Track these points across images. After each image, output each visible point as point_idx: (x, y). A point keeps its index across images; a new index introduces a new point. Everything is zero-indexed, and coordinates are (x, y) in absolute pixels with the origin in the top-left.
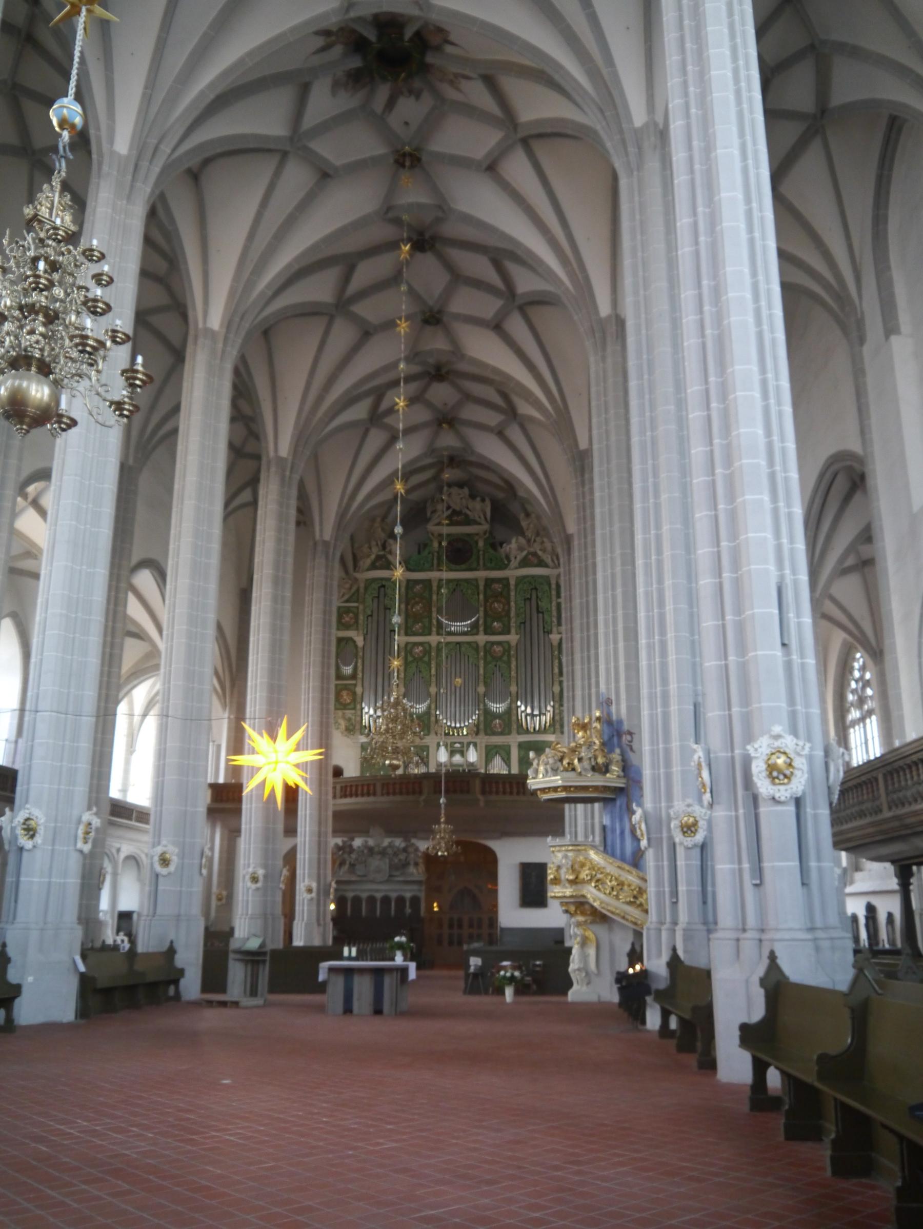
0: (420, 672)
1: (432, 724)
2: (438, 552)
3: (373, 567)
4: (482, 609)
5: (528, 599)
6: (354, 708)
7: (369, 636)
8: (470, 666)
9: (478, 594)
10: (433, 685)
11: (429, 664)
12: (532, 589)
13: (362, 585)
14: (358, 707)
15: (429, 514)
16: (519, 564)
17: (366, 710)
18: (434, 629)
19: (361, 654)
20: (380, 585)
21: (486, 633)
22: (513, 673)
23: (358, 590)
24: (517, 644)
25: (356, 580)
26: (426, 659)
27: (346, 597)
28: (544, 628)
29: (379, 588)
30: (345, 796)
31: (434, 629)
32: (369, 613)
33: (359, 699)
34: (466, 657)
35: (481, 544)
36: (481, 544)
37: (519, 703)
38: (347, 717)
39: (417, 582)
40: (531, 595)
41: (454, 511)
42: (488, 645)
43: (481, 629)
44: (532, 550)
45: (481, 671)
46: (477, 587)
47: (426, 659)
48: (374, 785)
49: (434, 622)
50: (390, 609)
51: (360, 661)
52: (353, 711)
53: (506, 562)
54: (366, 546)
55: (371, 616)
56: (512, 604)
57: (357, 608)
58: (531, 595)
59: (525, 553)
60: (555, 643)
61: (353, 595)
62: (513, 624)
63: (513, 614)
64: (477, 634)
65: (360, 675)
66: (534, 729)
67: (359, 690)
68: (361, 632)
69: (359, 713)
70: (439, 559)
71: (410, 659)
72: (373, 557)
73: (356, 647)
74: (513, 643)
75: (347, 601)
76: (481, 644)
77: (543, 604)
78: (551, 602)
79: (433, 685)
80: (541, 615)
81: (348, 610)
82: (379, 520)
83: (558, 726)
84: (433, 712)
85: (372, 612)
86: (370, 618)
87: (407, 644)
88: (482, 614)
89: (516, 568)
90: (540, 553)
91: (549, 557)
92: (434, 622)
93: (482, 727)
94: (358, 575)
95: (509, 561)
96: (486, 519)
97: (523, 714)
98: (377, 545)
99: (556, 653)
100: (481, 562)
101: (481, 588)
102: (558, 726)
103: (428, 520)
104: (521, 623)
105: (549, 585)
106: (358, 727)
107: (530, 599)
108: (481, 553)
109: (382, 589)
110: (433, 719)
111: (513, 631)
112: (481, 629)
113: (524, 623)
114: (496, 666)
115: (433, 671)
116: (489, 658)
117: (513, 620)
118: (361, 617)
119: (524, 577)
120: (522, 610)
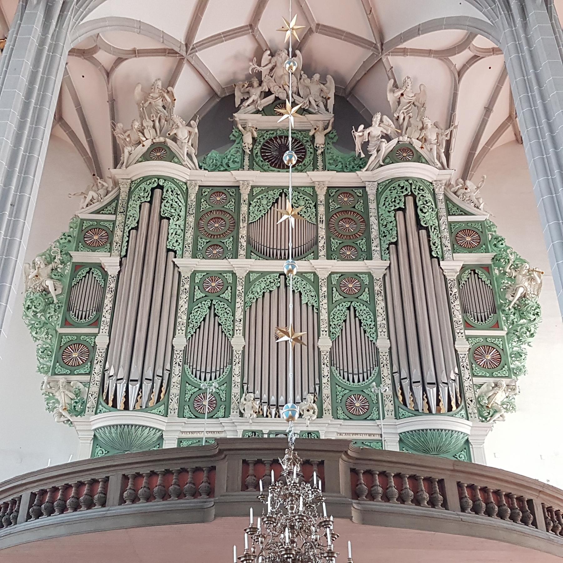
0: (215, 315)
1: (234, 399)
2: (251, 151)
3: (146, 157)
4: (322, 227)
5: (400, 209)
6: (89, 373)
7: (128, 262)
8: (304, 307)
9: (315, 206)
10: (239, 335)
11: (232, 303)
12: (405, 196)
13: (124, 190)
14: (98, 368)
15: (237, 102)
16: (383, 161)
17: (112, 372)
18: (242, 252)
19: (113, 285)
20: (156, 185)
21: (329, 257)
22: (381, 320)
23: (117, 198)
24: (385, 275)
25: (116, 184)
26: (227, 295)
27: (96, 206)
28: (431, 251)
29: (153, 190)
30: (39, 515)
31: (242, 252)
32: (134, 225)
33: (99, 356)
34: (297, 295)
35: (320, 140)
36: (320, 140)
37: (395, 369)
38: (73, 390)
39: (218, 190)
40: (405, 203)
41: (277, 98)
42: (335, 278)
43: (322, 253)
44: (405, 139)
45: (324, 316)
46: (314, 196)
47: (227, 295)
48: (107, 480)
49: (243, 242)
50: (169, 219)
51: (109, 296)
52: (86, 378)
53: (363, 155)
54: (137, 125)
55: (136, 228)
56: (373, 220)
57: (114, 222)
58: (405, 203)
59: (394, 142)
60: (452, 276)
61: (109, 204)
62: (375, 246)
63: (374, 233)
64: (316, 257)
65: (106, 317)
66: (430, 409)
67: (102, 341)
68: (115, 253)
69: (98, 378)
70: (252, 158)
71: (198, 294)
72: (148, 144)
73: (105, 274)
74: (378, 275)
75: (98, 212)
76: (323, 275)
77: (428, 218)
78: (438, 219)
79: (239, 335)
80: (423, 232)
81: (97, 227)
82: (160, 83)
83: (473, 408)
84: (237, 379)
85: (138, 223)
86: (134, 231)
87: (194, 273)
88: (322, 233)
89: (382, 166)
90: (417, 144)
91: (435, 147)
92: (243, 242)
93: (327, 405)
94: (118, 173)
95: (368, 156)
96: (326, 106)
97: (406, 383)
98: (154, 127)
99: (455, 290)
100: (320, 164)
101: (321, 197)
102: (473, 408)
103: (237, 110)
104: (390, 244)
105: (434, 195)
106: (91, 402)
107: (404, 210)
108: (319, 152)
109: (158, 191)
110: (236, 390)
111: (376, 255)
112: (322, 253)
113: (396, 243)
114: (349, 309)
115: (239, 314)
116: (337, 297)
117: (376, 242)
118: (118, 232)
119: (393, 180)
120: (390, 226)
